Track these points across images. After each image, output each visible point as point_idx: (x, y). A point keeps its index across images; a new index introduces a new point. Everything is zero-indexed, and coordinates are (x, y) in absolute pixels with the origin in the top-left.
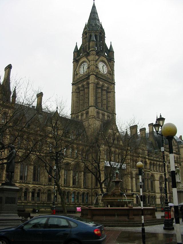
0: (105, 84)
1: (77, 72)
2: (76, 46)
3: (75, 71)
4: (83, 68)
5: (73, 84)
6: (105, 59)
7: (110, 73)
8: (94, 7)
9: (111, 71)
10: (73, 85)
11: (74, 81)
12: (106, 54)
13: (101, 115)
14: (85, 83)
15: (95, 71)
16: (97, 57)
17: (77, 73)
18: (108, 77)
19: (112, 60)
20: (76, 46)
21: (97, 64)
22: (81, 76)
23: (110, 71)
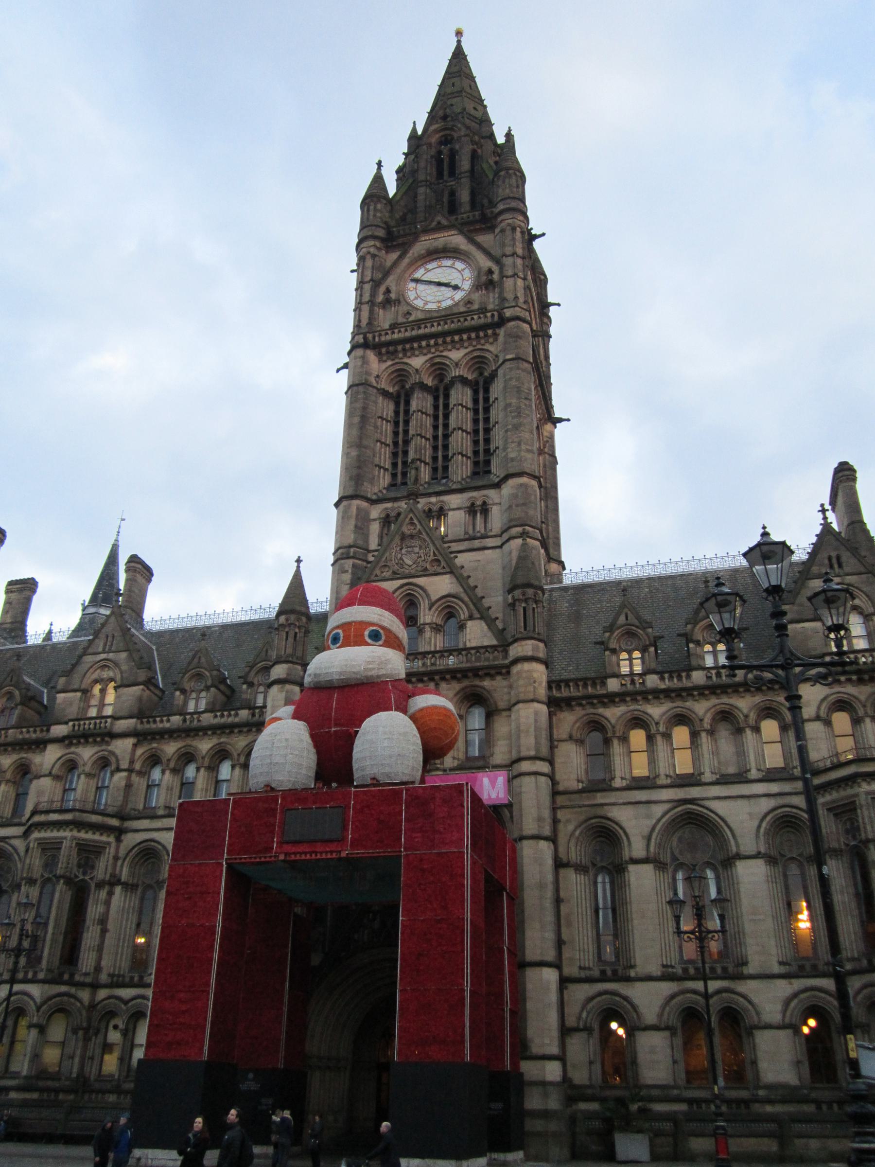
1: (388, 291)
2: (378, 180)
3: (376, 284)
4: (439, 284)
8: (459, 56)
14: (456, 355)
17: (393, 296)
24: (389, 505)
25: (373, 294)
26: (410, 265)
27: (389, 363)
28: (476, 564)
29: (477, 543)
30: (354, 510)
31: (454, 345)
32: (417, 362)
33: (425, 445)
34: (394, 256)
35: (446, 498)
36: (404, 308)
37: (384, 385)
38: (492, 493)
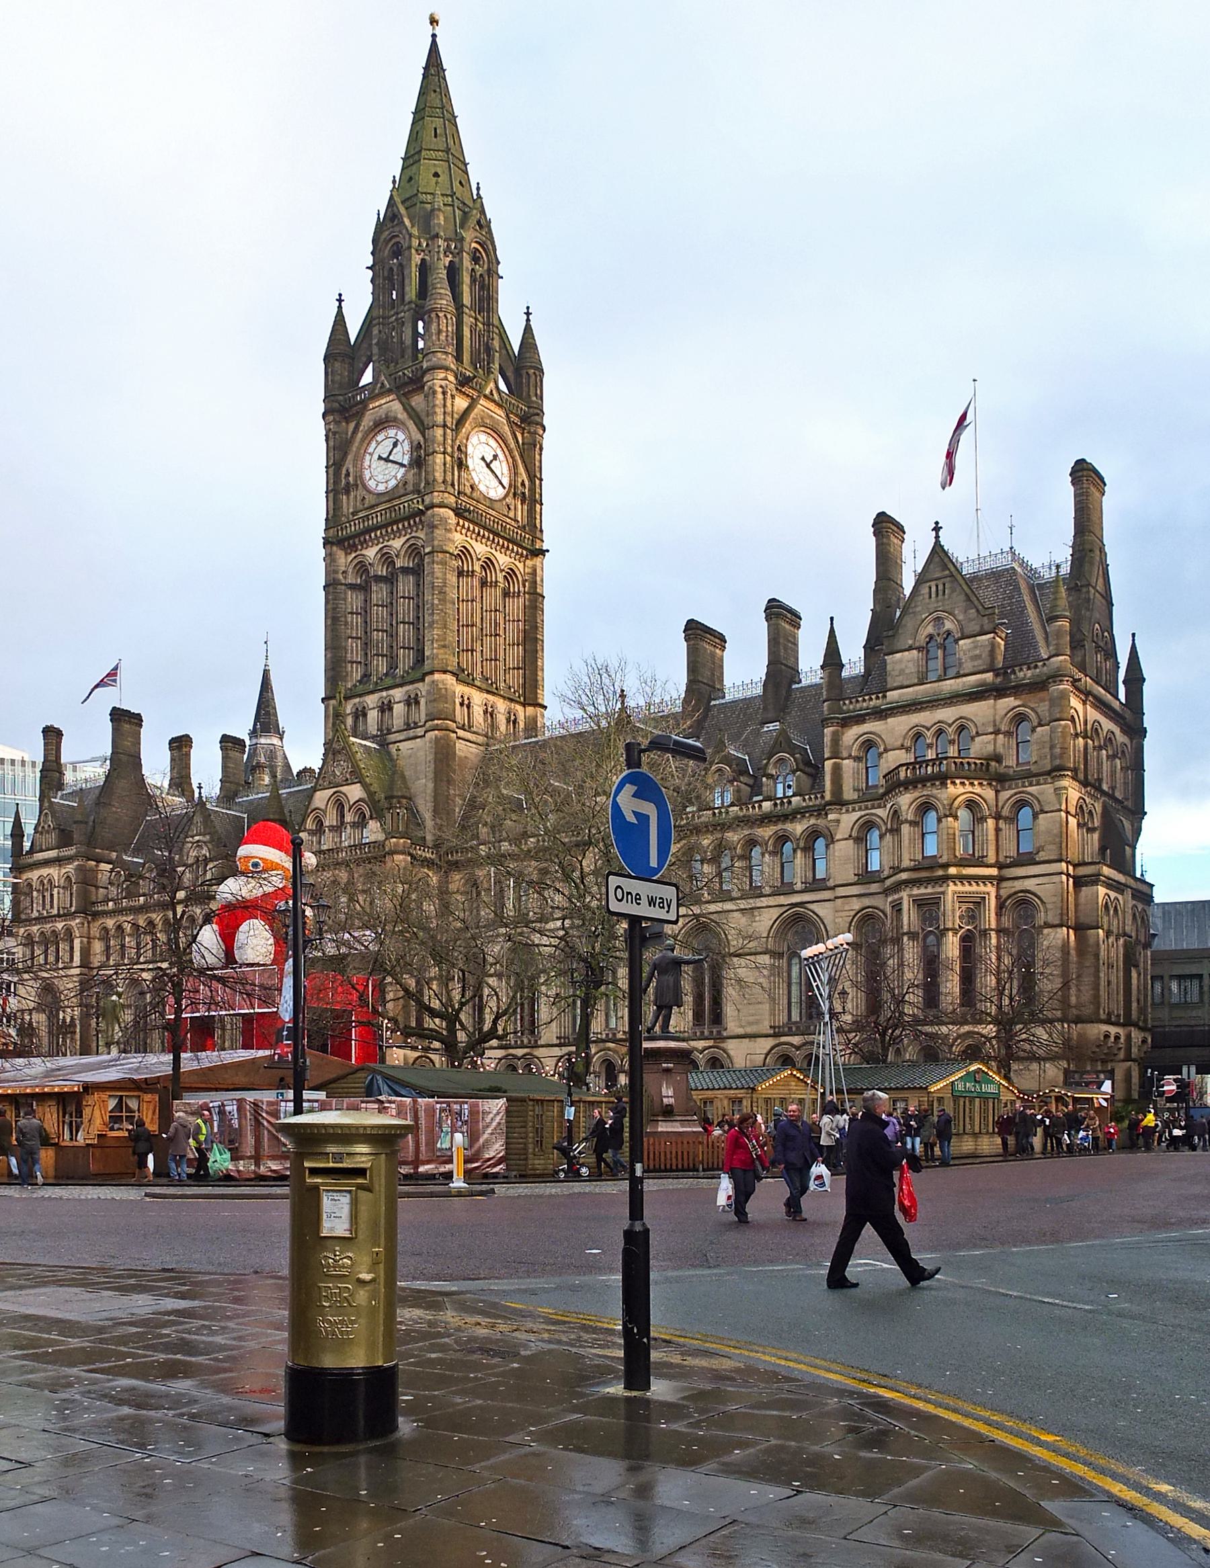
0: (497, 554)
2: (340, 321)
5: (327, 542)
6: (499, 415)
7: (524, 493)
8: (434, 66)
9: (527, 483)
10: (328, 546)
11: (332, 521)
12: (502, 386)
13: (478, 711)
14: (397, 543)
15: (453, 485)
16: (461, 403)
17: (351, 479)
18: (511, 514)
19: (537, 418)
20: (340, 321)
21: (463, 448)
22: (370, 500)
23: (523, 484)
24: (357, 700)
25: (337, 481)
26: (363, 440)
27: (353, 555)
28: (410, 751)
29: (411, 733)
30: (331, 708)
31: (397, 534)
32: (371, 553)
33: (383, 637)
34: (352, 425)
35: (391, 692)
36: (361, 492)
37: (351, 579)
38: (420, 685)
